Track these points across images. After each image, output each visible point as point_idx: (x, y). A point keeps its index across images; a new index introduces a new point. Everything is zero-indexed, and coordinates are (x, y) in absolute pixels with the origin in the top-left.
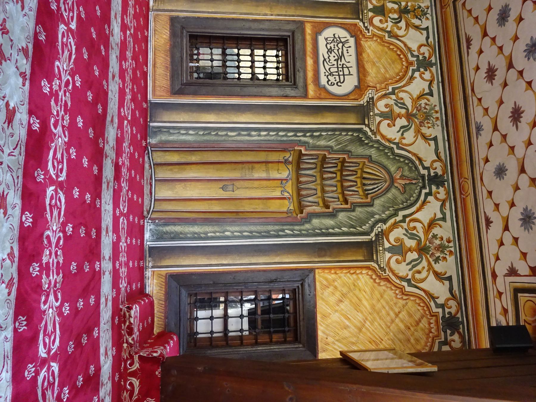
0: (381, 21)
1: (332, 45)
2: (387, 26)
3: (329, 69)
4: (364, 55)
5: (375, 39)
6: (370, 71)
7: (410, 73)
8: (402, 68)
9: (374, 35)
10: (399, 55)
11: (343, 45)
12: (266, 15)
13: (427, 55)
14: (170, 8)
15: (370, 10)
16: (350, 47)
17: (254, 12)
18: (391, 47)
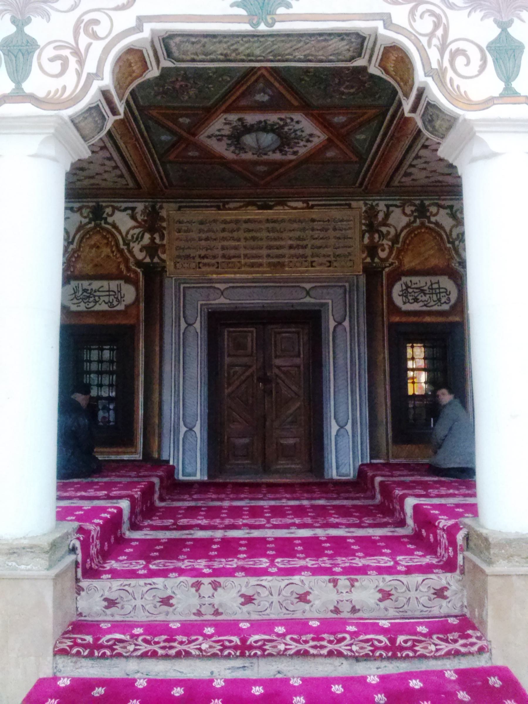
0: (383, 250)
1: (410, 298)
2: (387, 244)
3: (434, 301)
4: (418, 267)
5: (401, 257)
6: (433, 264)
7: (432, 226)
8: (428, 233)
9: (397, 257)
10: (416, 235)
11: (410, 287)
12: (384, 358)
13: (413, 208)
14: (384, 444)
15: (373, 259)
16: (411, 281)
17: (383, 368)
18: (408, 242)
